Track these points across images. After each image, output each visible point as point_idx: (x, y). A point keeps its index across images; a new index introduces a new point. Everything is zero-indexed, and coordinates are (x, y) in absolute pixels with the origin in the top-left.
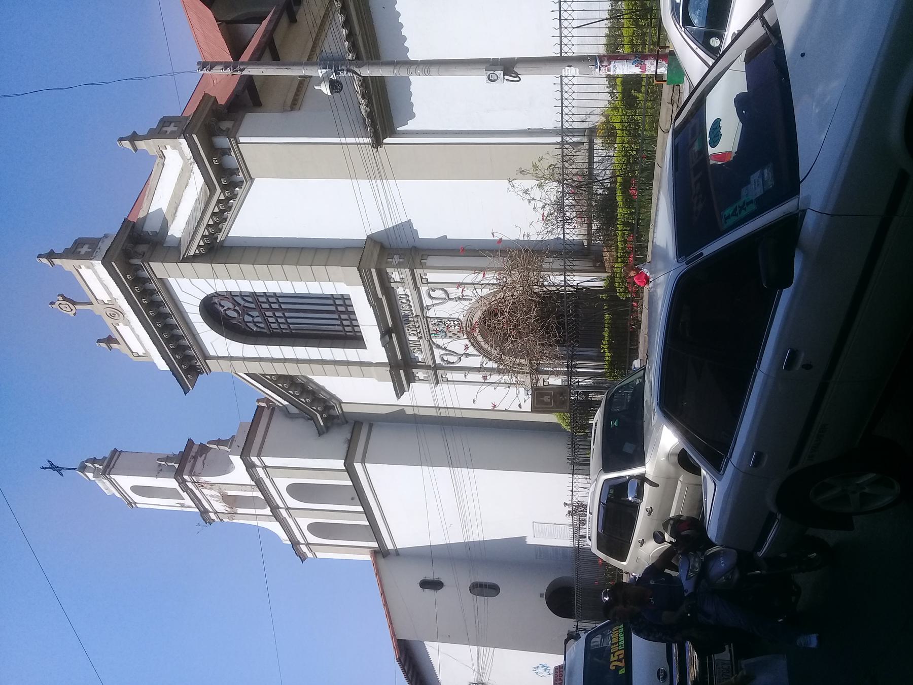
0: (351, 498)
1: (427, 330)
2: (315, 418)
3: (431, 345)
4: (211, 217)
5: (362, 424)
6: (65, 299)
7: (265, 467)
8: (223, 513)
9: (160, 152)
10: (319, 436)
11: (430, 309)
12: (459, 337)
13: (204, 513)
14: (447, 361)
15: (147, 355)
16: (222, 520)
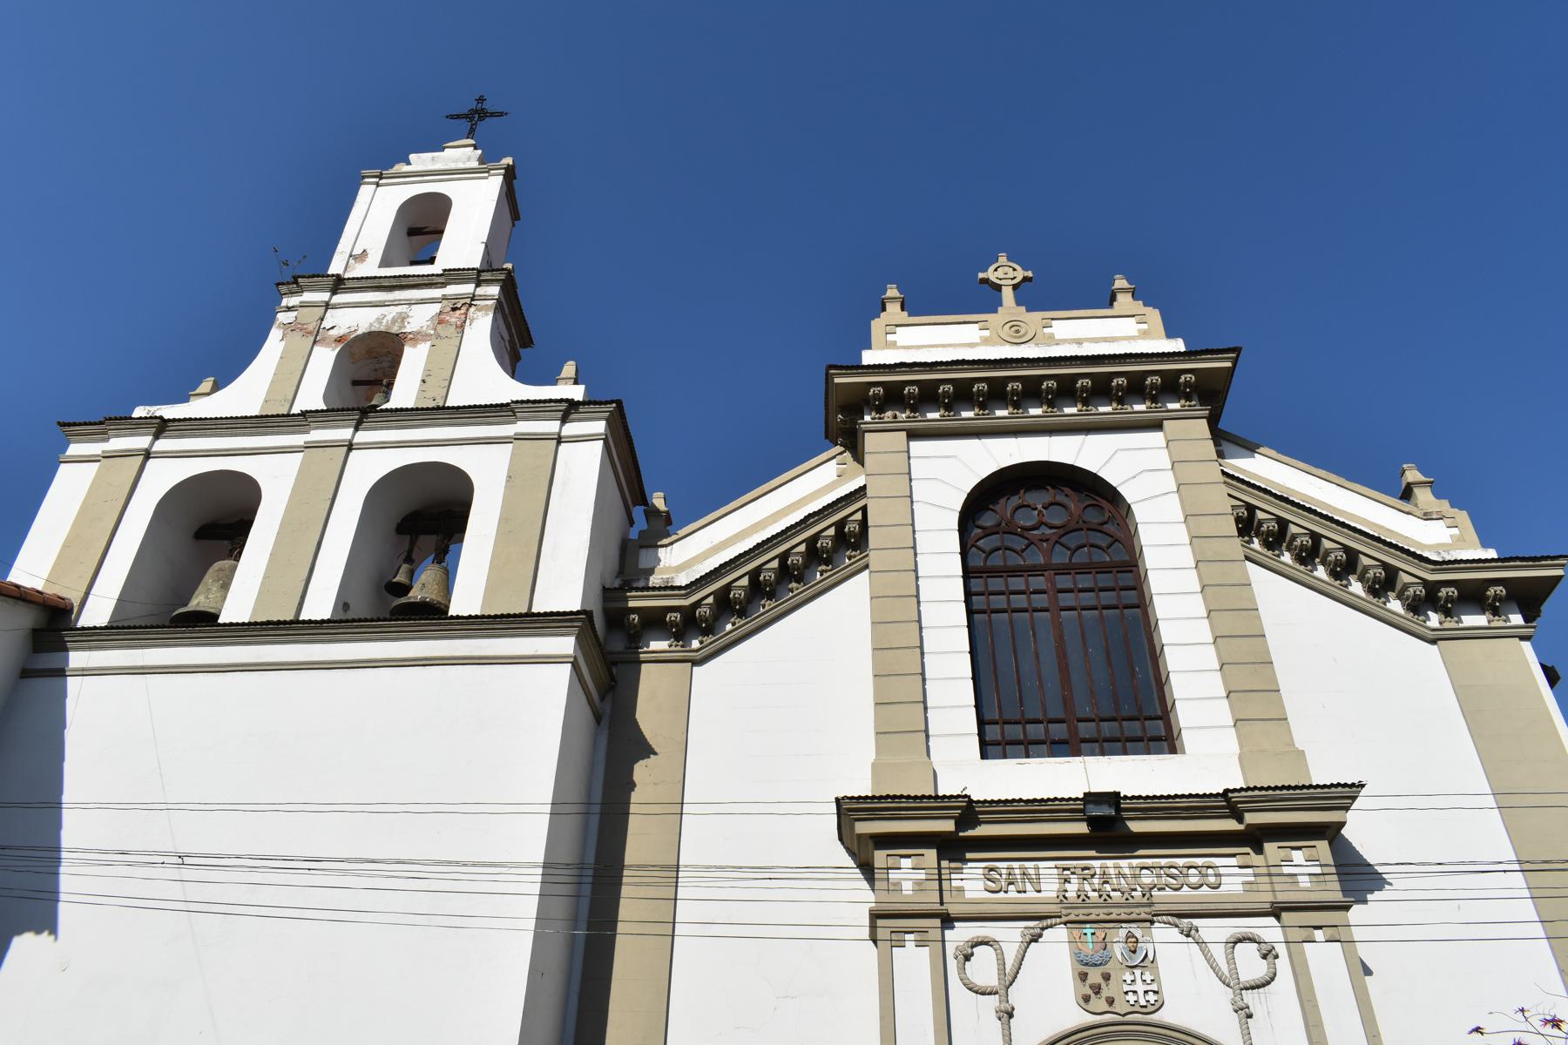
0: (349, 602)
1: (1103, 917)
2: (683, 592)
3: (1038, 920)
4: (1346, 549)
5: (602, 699)
6: (1025, 279)
7: (559, 440)
8: (322, 320)
9: (1439, 517)
10: (604, 587)
11: (1188, 936)
12: (1087, 999)
13: (338, 284)
14: (972, 954)
15: (893, 345)
16: (289, 309)
